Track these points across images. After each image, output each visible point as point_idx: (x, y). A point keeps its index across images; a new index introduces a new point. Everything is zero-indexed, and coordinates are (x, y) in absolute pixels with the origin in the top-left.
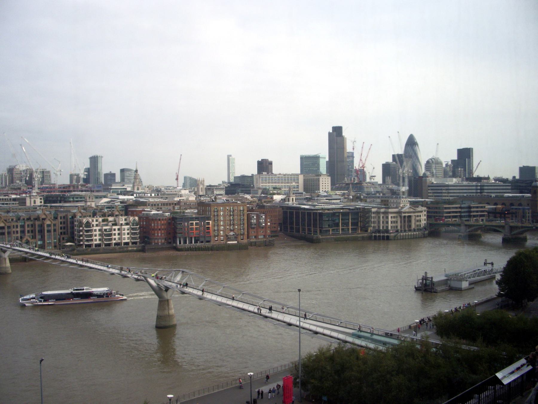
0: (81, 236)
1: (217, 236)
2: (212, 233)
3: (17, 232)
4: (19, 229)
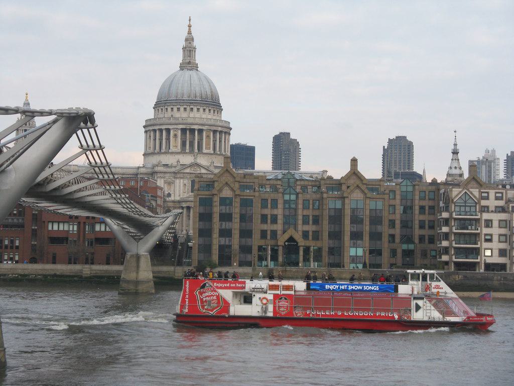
3: (274, 220)
4: (279, 212)
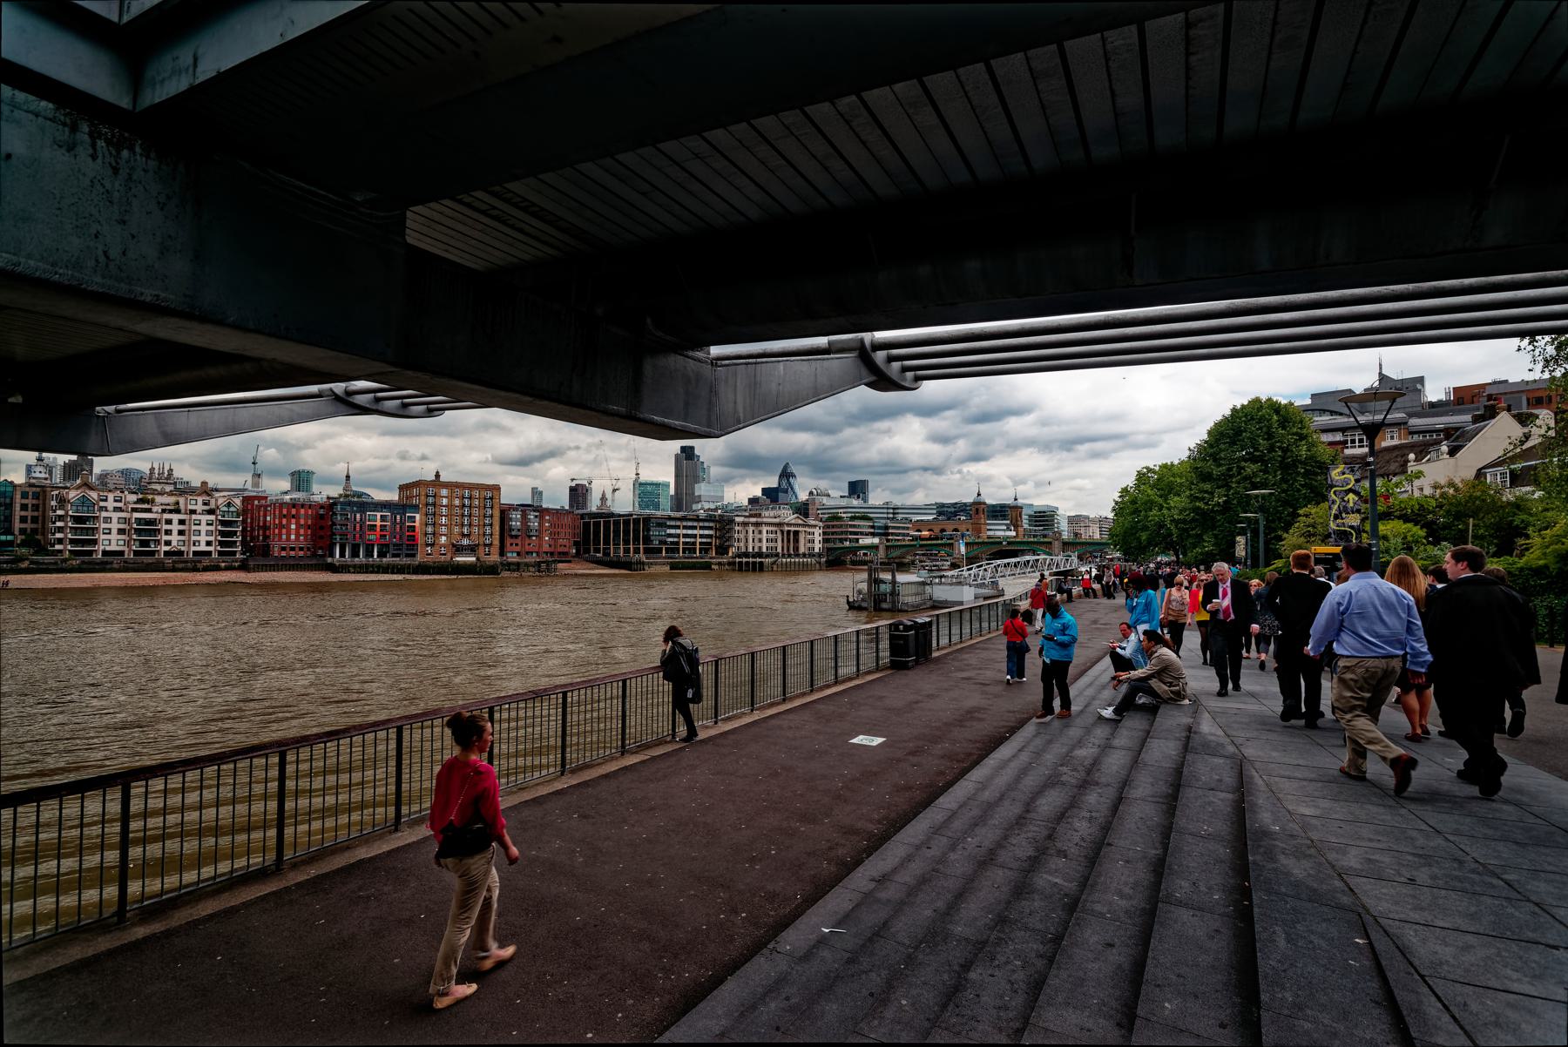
0: (60, 530)
1: (432, 545)
2: (420, 541)
